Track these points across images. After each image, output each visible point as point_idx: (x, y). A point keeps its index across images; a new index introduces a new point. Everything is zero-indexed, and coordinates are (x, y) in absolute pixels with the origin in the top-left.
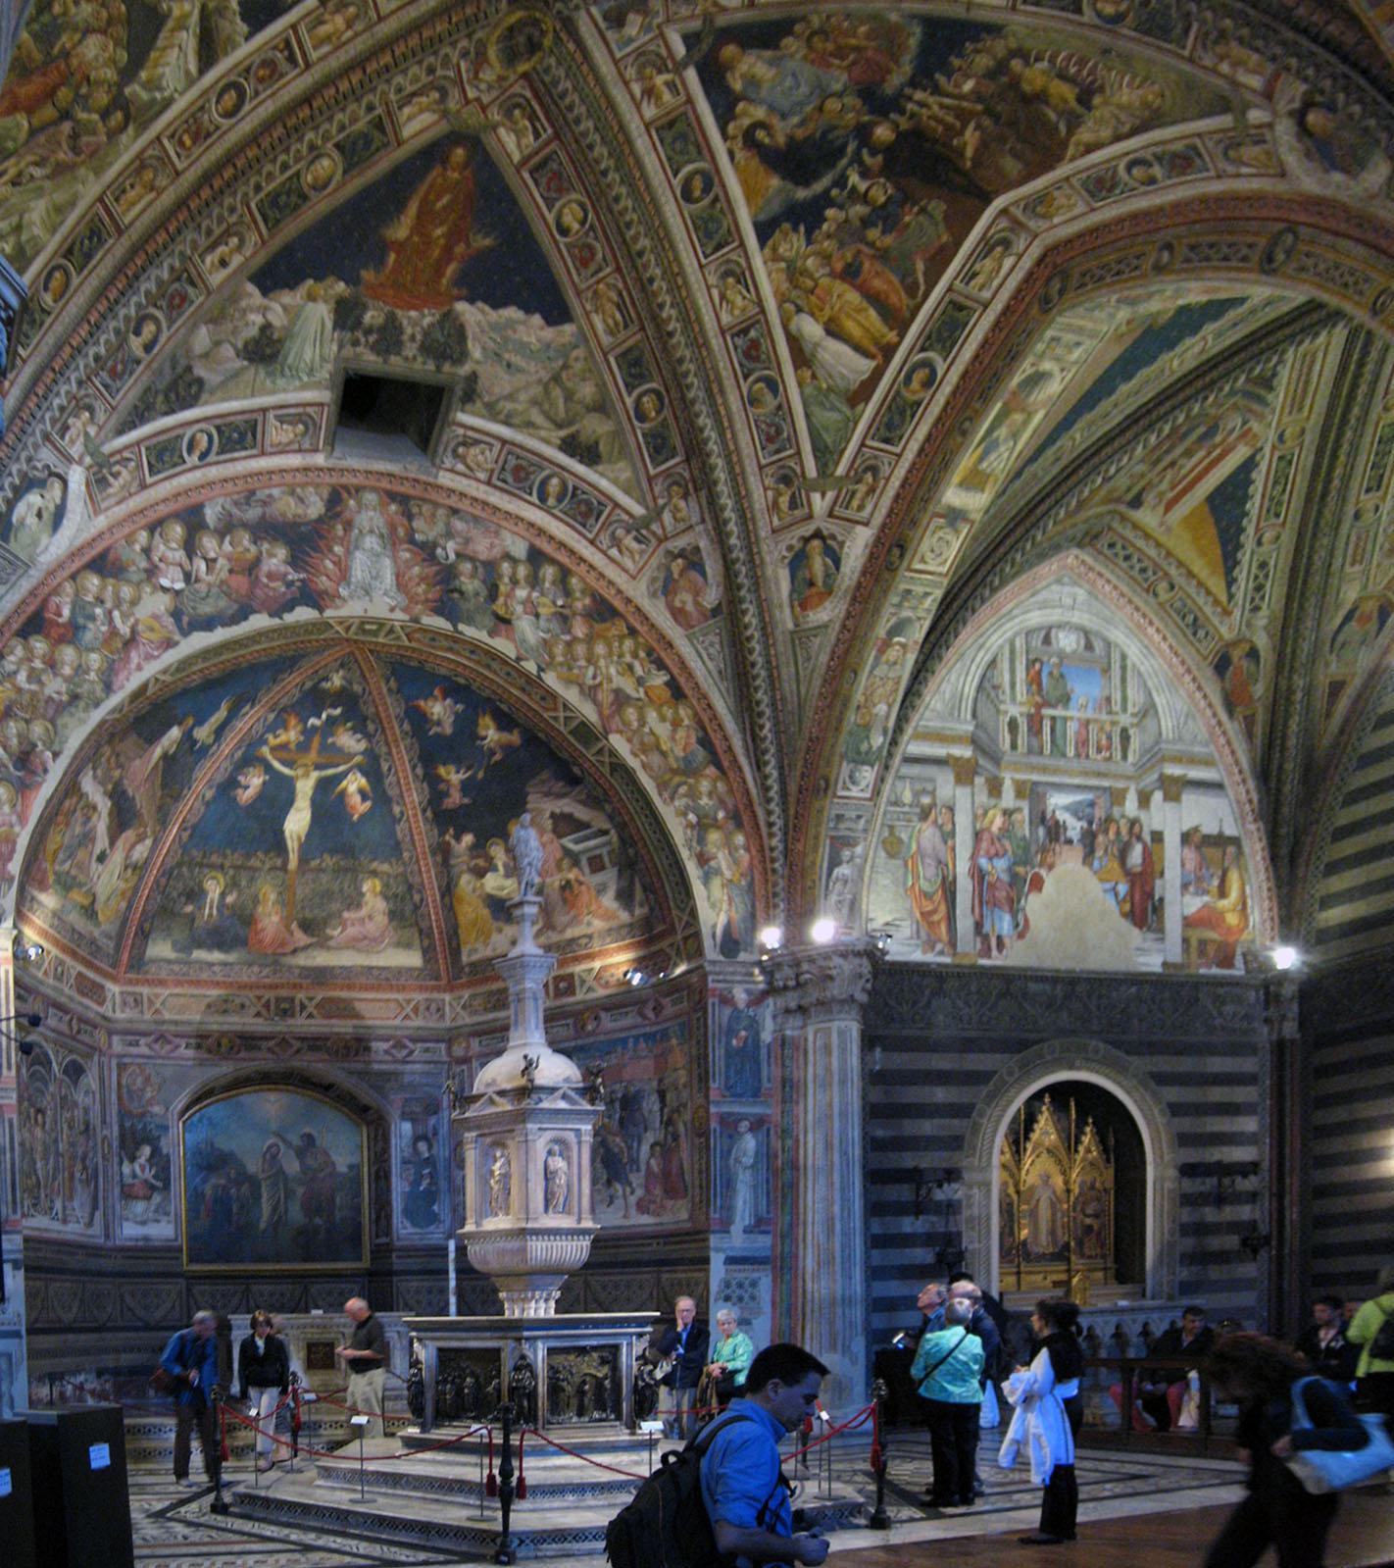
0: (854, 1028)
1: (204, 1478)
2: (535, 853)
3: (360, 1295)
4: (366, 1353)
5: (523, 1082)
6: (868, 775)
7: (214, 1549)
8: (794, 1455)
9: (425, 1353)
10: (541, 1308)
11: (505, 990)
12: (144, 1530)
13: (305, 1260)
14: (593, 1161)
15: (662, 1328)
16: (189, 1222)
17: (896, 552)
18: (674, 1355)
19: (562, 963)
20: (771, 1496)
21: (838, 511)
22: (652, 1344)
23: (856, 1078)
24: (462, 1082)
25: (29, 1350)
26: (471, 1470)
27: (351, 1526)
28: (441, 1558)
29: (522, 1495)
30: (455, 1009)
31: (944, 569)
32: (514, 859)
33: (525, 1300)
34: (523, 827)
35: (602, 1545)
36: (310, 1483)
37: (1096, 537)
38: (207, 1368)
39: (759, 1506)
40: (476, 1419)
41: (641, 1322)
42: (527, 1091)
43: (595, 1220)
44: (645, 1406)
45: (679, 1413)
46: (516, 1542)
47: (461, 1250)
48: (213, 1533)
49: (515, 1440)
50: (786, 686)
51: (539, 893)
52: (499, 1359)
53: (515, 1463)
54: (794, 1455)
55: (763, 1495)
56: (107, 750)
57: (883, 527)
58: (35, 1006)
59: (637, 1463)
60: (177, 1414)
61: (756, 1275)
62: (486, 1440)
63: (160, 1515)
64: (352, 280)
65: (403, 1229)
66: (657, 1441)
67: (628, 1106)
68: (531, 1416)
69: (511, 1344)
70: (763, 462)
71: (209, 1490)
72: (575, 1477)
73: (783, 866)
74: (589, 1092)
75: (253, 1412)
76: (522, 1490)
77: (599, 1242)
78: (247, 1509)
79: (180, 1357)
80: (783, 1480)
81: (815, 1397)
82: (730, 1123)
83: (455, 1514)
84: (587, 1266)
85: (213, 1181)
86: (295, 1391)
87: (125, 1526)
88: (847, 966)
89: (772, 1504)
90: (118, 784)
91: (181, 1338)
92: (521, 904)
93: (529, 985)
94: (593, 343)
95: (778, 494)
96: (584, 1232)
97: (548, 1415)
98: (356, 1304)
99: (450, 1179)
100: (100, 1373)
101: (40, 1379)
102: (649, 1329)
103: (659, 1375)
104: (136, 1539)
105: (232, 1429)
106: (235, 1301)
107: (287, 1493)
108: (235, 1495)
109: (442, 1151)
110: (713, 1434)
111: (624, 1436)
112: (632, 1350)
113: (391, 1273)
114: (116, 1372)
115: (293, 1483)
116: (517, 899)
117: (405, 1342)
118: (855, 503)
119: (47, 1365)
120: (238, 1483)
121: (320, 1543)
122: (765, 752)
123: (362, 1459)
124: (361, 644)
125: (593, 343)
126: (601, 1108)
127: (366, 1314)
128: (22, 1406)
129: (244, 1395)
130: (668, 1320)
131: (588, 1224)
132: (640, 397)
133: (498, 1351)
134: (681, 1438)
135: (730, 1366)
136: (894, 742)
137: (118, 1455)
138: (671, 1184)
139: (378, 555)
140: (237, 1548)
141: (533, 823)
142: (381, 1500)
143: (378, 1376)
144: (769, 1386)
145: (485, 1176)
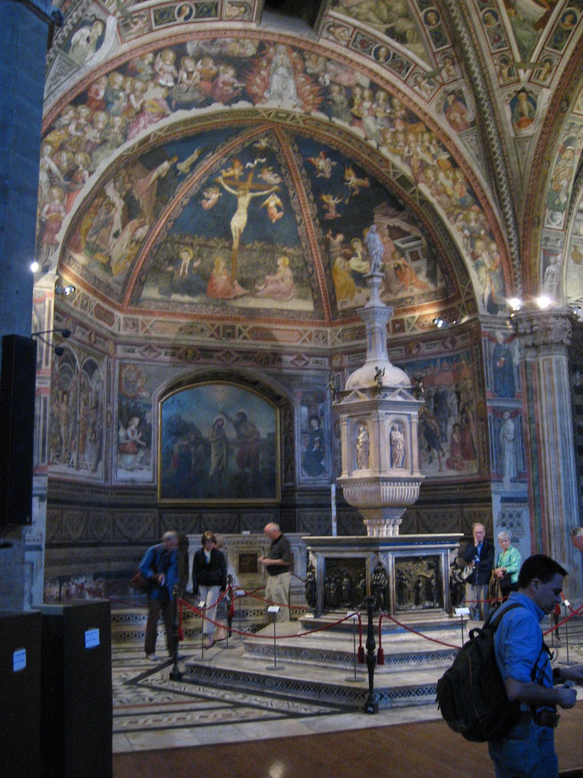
0: (564, 360)
1: (166, 654)
2: (379, 248)
3: (274, 521)
4: (278, 561)
5: (375, 384)
6: (560, 217)
7: (170, 708)
8: (551, 630)
9: (317, 561)
10: (390, 531)
11: (362, 328)
12: (122, 694)
13: (239, 497)
14: (419, 435)
15: (465, 544)
16: (163, 470)
17: (564, 104)
18: (473, 562)
19: (397, 313)
20: (538, 660)
21: (533, 79)
22: (460, 555)
23: (567, 390)
24: (338, 383)
25: (46, 560)
26: (347, 644)
27: (268, 688)
28: (328, 710)
29: (381, 662)
30: (334, 337)
32: (367, 250)
33: (380, 525)
34: (371, 232)
35: (434, 697)
36: (239, 656)
38: (171, 572)
39: (532, 666)
40: (351, 607)
41: (452, 540)
42: (378, 389)
43: (422, 472)
44: (457, 599)
45: (479, 602)
46: (378, 696)
47: (339, 491)
48: (171, 696)
49: (376, 622)
50: (513, 166)
51: (382, 271)
52: (364, 566)
53: (376, 639)
54: (551, 630)
55: (533, 658)
56: (123, 172)
57: (557, 90)
58: (67, 325)
59: (454, 637)
60: (149, 606)
61: (520, 509)
62: (357, 623)
63: (132, 683)
65: (302, 477)
66: (466, 621)
67: (439, 399)
68: (385, 605)
69: (372, 555)
70: (493, 52)
71: (169, 663)
72: (415, 648)
73: (519, 263)
74: (415, 391)
75: (202, 604)
76: (381, 659)
77: (426, 487)
78: (194, 677)
79: (152, 565)
80: (545, 648)
81: (561, 590)
82: (498, 413)
83: (338, 677)
84: (418, 502)
85: (179, 442)
86: (230, 588)
87: (107, 691)
88: (559, 323)
89: (540, 665)
90: (129, 192)
91: (154, 550)
92: (371, 277)
93: (377, 324)
95: (502, 68)
96: (415, 480)
97: (396, 605)
98: (272, 527)
99: (332, 444)
100: (96, 577)
101: (53, 581)
102: (457, 545)
103: (465, 576)
104: (115, 701)
105: (187, 616)
106: (191, 525)
107: (224, 664)
108: (187, 666)
109: (326, 426)
110: (500, 617)
111: (445, 619)
112: (448, 559)
113: (295, 506)
114: (107, 575)
115: (228, 656)
116: (369, 274)
117: (304, 554)
118: (542, 77)
119: (58, 570)
120: (189, 657)
121: (246, 701)
122: (504, 200)
123: (275, 638)
124: (276, 124)
126: (423, 401)
127: (278, 534)
128: (38, 601)
129: (196, 591)
130: (468, 539)
131: (417, 475)
133: (363, 560)
134: (481, 619)
135: (508, 570)
136: (572, 201)
137: (106, 638)
138: (466, 450)
139: (286, 78)
140: (187, 707)
141: (377, 230)
142: (288, 668)
143: (286, 577)
144: (533, 584)
145: (354, 443)
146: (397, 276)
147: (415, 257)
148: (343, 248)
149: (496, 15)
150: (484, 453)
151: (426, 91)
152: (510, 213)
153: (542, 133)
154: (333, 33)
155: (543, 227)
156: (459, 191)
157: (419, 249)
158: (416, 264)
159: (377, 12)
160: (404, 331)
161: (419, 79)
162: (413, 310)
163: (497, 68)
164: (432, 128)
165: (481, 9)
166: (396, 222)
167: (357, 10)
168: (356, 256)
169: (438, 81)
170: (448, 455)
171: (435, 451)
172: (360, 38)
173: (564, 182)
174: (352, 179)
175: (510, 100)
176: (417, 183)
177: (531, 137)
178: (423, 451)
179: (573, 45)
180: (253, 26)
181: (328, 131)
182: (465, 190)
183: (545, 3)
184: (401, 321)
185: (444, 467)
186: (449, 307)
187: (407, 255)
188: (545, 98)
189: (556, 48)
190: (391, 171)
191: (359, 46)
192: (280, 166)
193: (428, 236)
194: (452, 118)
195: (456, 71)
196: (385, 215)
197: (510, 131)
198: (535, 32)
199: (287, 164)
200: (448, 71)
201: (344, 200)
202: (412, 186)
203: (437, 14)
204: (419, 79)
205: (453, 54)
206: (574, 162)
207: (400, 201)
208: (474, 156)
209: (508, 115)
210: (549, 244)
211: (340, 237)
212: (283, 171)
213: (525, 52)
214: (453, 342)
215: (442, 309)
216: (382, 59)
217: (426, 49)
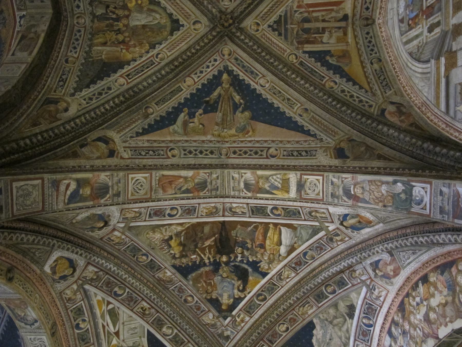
21: (330, 220)
31: (320, 178)
37: (367, 19)
70: (330, 249)
94: (317, 312)
118: (324, 215)
125: (317, 312)
132: (328, 293)
149: (305, 254)
151: (382, 291)
152: (443, 236)
155: (429, 216)
156: (442, 286)
159: (340, 325)
161: (374, 296)
163: (339, 243)
164: (406, 291)
165: (307, 263)
169: (370, 283)
172: (361, 337)
173: (384, 188)
175: (356, 232)
176: (437, 338)
177: (372, 213)
182: (440, 277)
183: (278, 229)
189: (299, 213)
191: (367, 338)
194: (392, 273)
195: (359, 269)
197: (380, 227)
198: (299, 228)
203: (326, 287)
204: (374, 296)
205: (348, 271)
206: (363, 181)
208: (415, 256)
209: (367, 230)
210: (447, 208)
217: (352, 291)
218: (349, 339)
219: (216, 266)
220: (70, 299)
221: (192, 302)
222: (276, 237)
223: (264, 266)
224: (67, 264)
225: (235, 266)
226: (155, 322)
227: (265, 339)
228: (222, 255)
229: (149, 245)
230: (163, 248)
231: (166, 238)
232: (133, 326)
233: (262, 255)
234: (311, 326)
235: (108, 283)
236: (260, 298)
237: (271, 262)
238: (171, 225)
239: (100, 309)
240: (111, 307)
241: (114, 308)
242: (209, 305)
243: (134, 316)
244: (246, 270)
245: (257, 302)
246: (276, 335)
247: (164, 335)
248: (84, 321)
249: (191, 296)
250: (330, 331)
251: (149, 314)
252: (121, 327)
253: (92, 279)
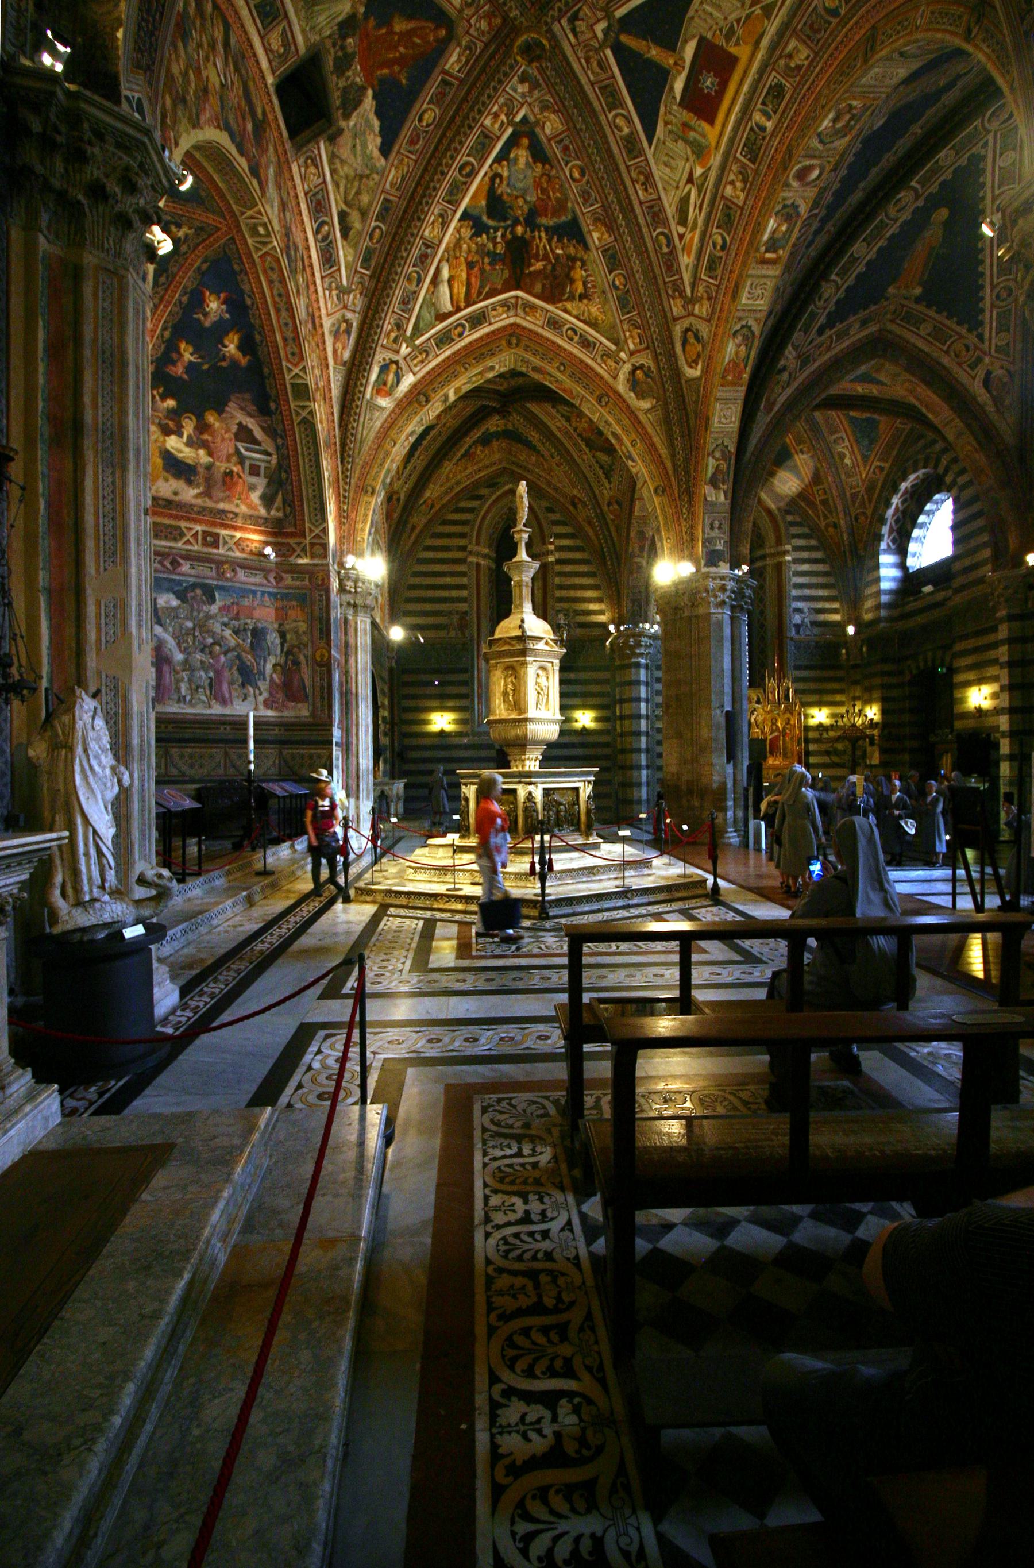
17: (423, 399)
57: (419, 382)
64: (366, 16)
95: (392, 330)
146: (224, 483)
147: (254, 471)
148: (167, 417)
149: (420, 281)
150: (322, 697)
153: (393, 411)
154: (307, 167)
157: (263, 465)
158: (253, 480)
160: (217, 547)
162: (235, 528)
166: (251, 423)
167: (338, 166)
168: (180, 435)
170: (265, 695)
171: (251, 689)
172: (319, 197)
174: (231, 347)
177: (383, 409)
178: (236, 686)
179: (448, 353)
180: (270, 80)
181: (271, 282)
184: (216, 536)
185: (261, 707)
186: (280, 540)
187: (247, 463)
188: (408, 381)
190: (296, 371)
192: (166, 271)
193: (283, 458)
196: (242, 409)
199: (174, 276)
200: (355, 297)
201: (202, 364)
202: (309, 399)
207: (273, 406)
209: (373, 377)
211: (171, 403)
212: (163, 279)
213: (417, 331)
214: (279, 579)
215: (270, 539)
216: (319, 237)
218: (333, 172)
219: (530, 221)
220: (709, 299)
221: (573, 166)
222: (455, 291)
223: (467, 232)
224: (688, 348)
225: (505, 219)
226: (636, 153)
227: (456, 82)
228: (522, 237)
229: (606, 301)
230: (594, 287)
231: (585, 301)
232: (667, 171)
233: (469, 251)
234: (385, 150)
235: (669, 268)
236: (468, 169)
237: (458, 244)
238: (577, 318)
239: (692, 238)
240: (681, 230)
241: (679, 223)
242: (548, 151)
243: (660, 188)
244: (490, 216)
245: (472, 159)
246: (438, 99)
247: (629, 120)
248: (714, 245)
249: (574, 180)
250: (359, 159)
251: (640, 173)
252: (681, 184)
253: (681, 296)
